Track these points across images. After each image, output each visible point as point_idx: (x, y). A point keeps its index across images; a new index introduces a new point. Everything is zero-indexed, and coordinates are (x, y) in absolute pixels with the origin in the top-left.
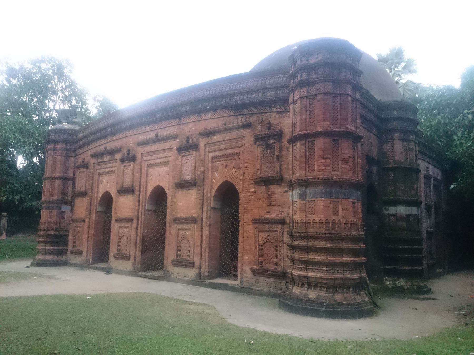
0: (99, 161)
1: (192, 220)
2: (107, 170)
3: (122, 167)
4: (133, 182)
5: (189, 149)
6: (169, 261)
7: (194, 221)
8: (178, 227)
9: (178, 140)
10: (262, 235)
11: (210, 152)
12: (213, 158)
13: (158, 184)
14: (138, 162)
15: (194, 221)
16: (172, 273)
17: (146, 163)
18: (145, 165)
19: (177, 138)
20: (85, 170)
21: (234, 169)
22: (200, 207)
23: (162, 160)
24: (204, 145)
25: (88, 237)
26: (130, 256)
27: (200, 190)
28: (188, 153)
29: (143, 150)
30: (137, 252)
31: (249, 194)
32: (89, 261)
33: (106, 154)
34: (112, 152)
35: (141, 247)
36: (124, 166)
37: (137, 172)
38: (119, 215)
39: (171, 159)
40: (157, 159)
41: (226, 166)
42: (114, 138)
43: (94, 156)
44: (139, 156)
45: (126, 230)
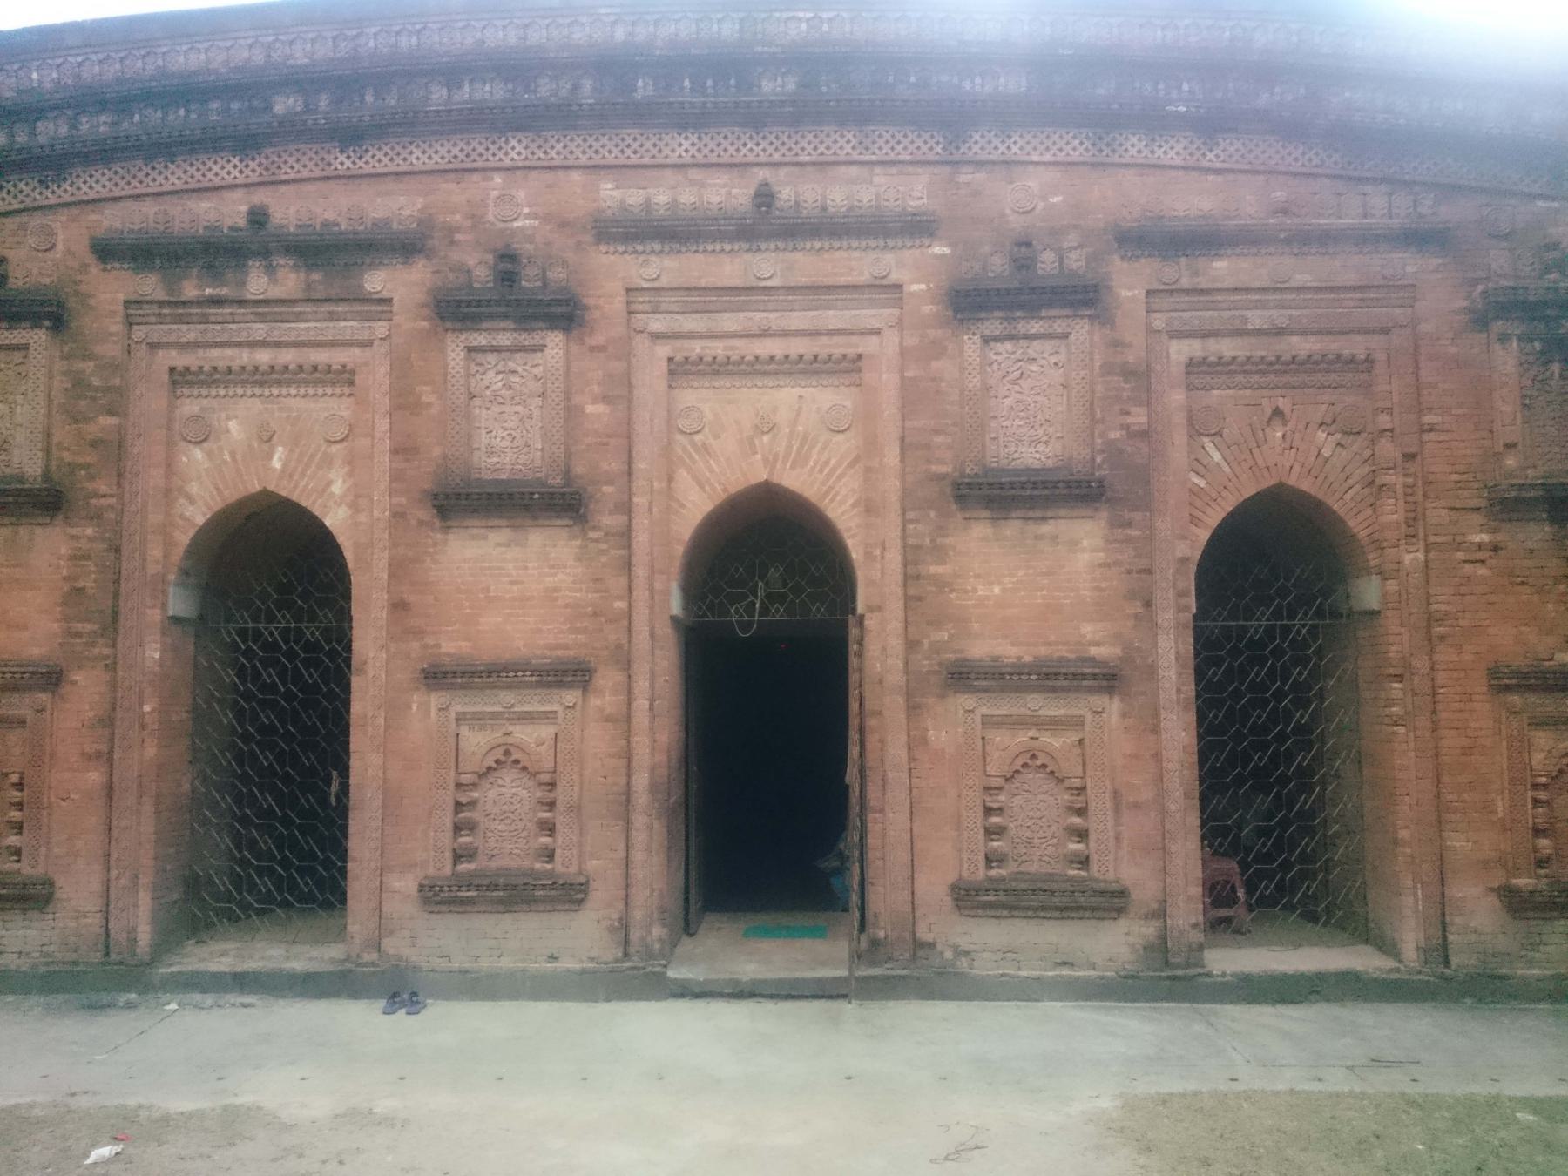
1: (1094, 677)
2: (264, 357)
4: (569, 454)
5: (1050, 305)
6: (934, 886)
7: (1108, 679)
8: (985, 710)
9: (940, 249)
10: (1542, 738)
12: (1192, 366)
13: (763, 476)
14: (599, 339)
15: (1108, 679)
16: (960, 953)
17: (663, 350)
18: (652, 362)
19: (931, 234)
21: (1321, 435)
22: (1137, 607)
23: (797, 347)
24: (1140, 293)
25: (110, 788)
27: (1129, 524)
28: (1035, 327)
29: (651, 272)
30: (638, 856)
31: (1460, 555)
32: (133, 941)
33: (265, 253)
34: (333, 255)
35: (659, 827)
36: (471, 350)
37: (605, 399)
38: (451, 646)
39: (869, 345)
40: (765, 334)
41: (1277, 412)
42: (343, 162)
43: (106, 251)
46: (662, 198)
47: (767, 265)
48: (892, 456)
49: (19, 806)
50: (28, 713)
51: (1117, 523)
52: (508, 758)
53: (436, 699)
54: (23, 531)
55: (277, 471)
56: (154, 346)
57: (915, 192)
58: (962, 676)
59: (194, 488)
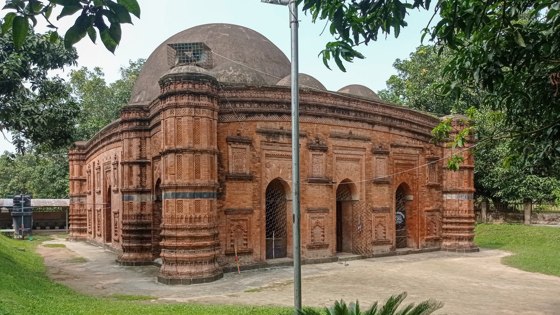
0: (271, 140)
2: (280, 153)
3: (311, 156)
11: (395, 159)
14: (329, 154)
17: (336, 156)
20: (248, 147)
23: (353, 157)
26: (328, 245)
28: (382, 157)
38: (309, 206)
39: (361, 157)
40: (349, 154)
44: (330, 148)
45: (321, 220)
46: (337, 131)
47: (350, 143)
48: (364, 175)
49: (246, 236)
50: (247, 218)
51: (390, 187)
52: (317, 224)
53: (308, 215)
54: (245, 184)
55: (279, 174)
56: (263, 149)
57: (367, 134)
58: (374, 210)
59: (268, 176)
